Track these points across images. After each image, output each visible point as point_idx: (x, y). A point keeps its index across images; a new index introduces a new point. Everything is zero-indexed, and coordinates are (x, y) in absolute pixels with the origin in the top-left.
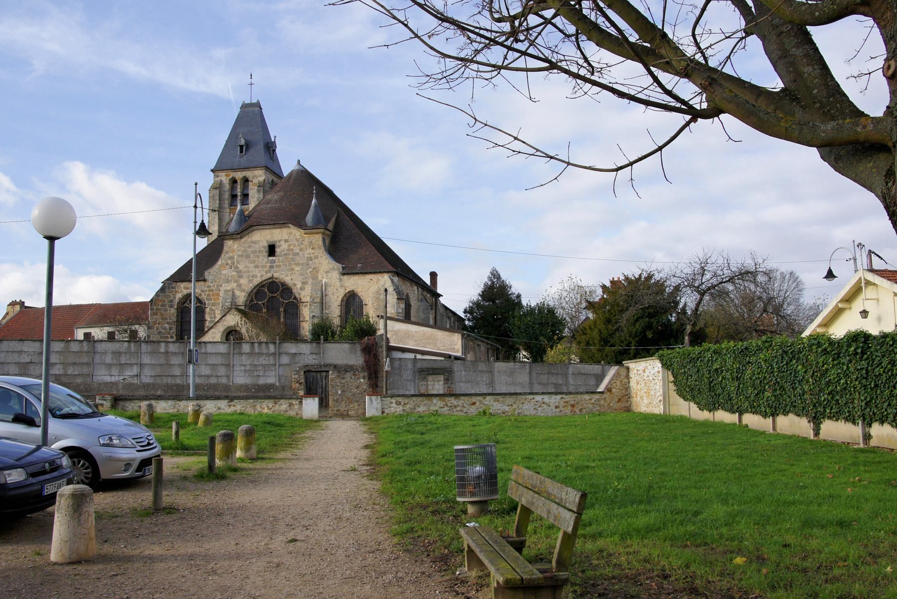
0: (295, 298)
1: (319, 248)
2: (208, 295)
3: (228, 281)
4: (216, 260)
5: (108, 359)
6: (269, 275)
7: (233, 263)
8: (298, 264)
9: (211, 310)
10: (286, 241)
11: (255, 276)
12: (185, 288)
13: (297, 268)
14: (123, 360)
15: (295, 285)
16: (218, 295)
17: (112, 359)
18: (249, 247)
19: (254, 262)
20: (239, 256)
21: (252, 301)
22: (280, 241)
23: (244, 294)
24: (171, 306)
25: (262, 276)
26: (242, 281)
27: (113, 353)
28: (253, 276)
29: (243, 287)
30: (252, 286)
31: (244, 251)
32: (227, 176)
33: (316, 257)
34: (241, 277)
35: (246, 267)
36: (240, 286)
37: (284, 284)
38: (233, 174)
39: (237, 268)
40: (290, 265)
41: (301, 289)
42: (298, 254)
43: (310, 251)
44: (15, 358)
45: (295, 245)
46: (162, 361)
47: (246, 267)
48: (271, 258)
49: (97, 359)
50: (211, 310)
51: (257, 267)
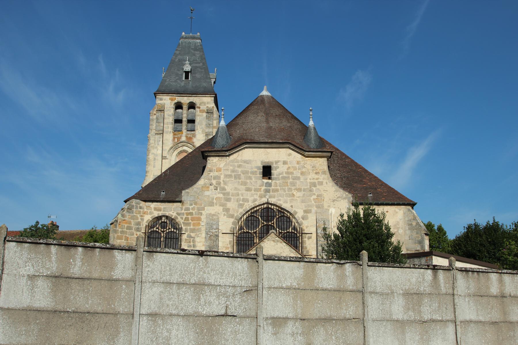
0: (294, 228)
1: (324, 173)
2: (187, 219)
3: (211, 204)
4: (198, 179)
5: (398, 309)
6: (264, 200)
7: (219, 184)
8: (299, 190)
9: (189, 236)
10: (285, 163)
11: (247, 201)
12: (155, 209)
13: (297, 194)
14: (428, 310)
15: (296, 213)
16: (199, 219)
17: (407, 309)
18: (239, 166)
19: (245, 184)
20: (226, 176)
21: (241, 228)
22: (277, 162)
23: (232, 220)
24: (138, 230)
25: (255, 200)
26: (229, 205)
27: (407, 294)
28: (244, 200)
29: (231, 212)
30: (241, 211)
31: (233, 171)
32: (172, 100)
33: (321, 183)
34: (229, 200)
35: (236, 189)
36: (227, 210)
37: (282, 211)
38: (178, 99)
39: (224, 189)
40: (290, 190)
41: (303, 218)
42: (299, 178)
43: (313, 175)
44: (186, 302)
45: (295, 168)
46: (495, 315)
47: (236, 189)
48: (266, 181)
49: (374, 306)
50: (189, 236)
51: (248, 190)
